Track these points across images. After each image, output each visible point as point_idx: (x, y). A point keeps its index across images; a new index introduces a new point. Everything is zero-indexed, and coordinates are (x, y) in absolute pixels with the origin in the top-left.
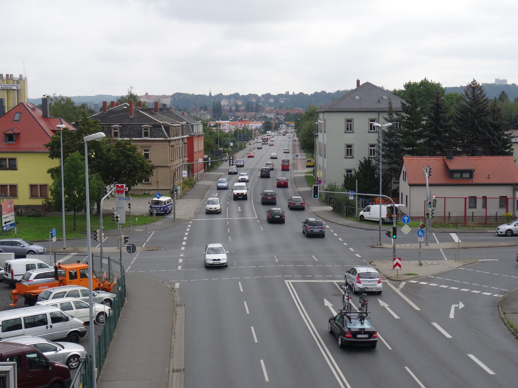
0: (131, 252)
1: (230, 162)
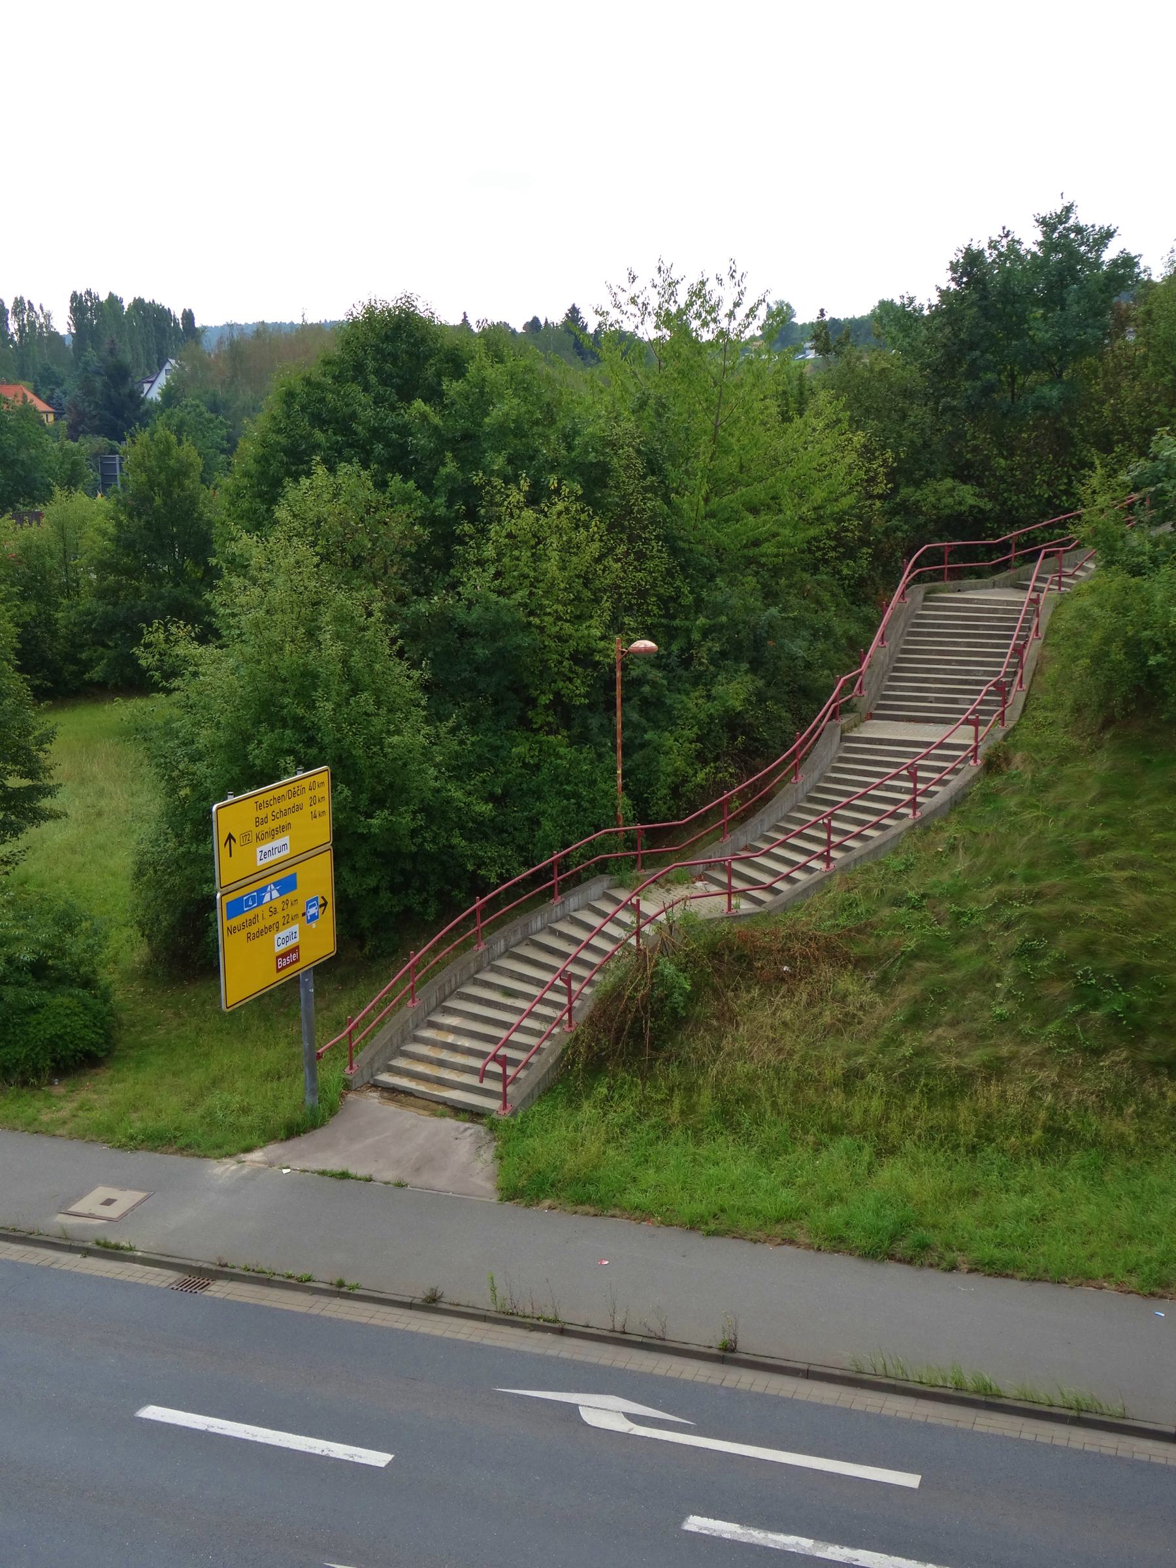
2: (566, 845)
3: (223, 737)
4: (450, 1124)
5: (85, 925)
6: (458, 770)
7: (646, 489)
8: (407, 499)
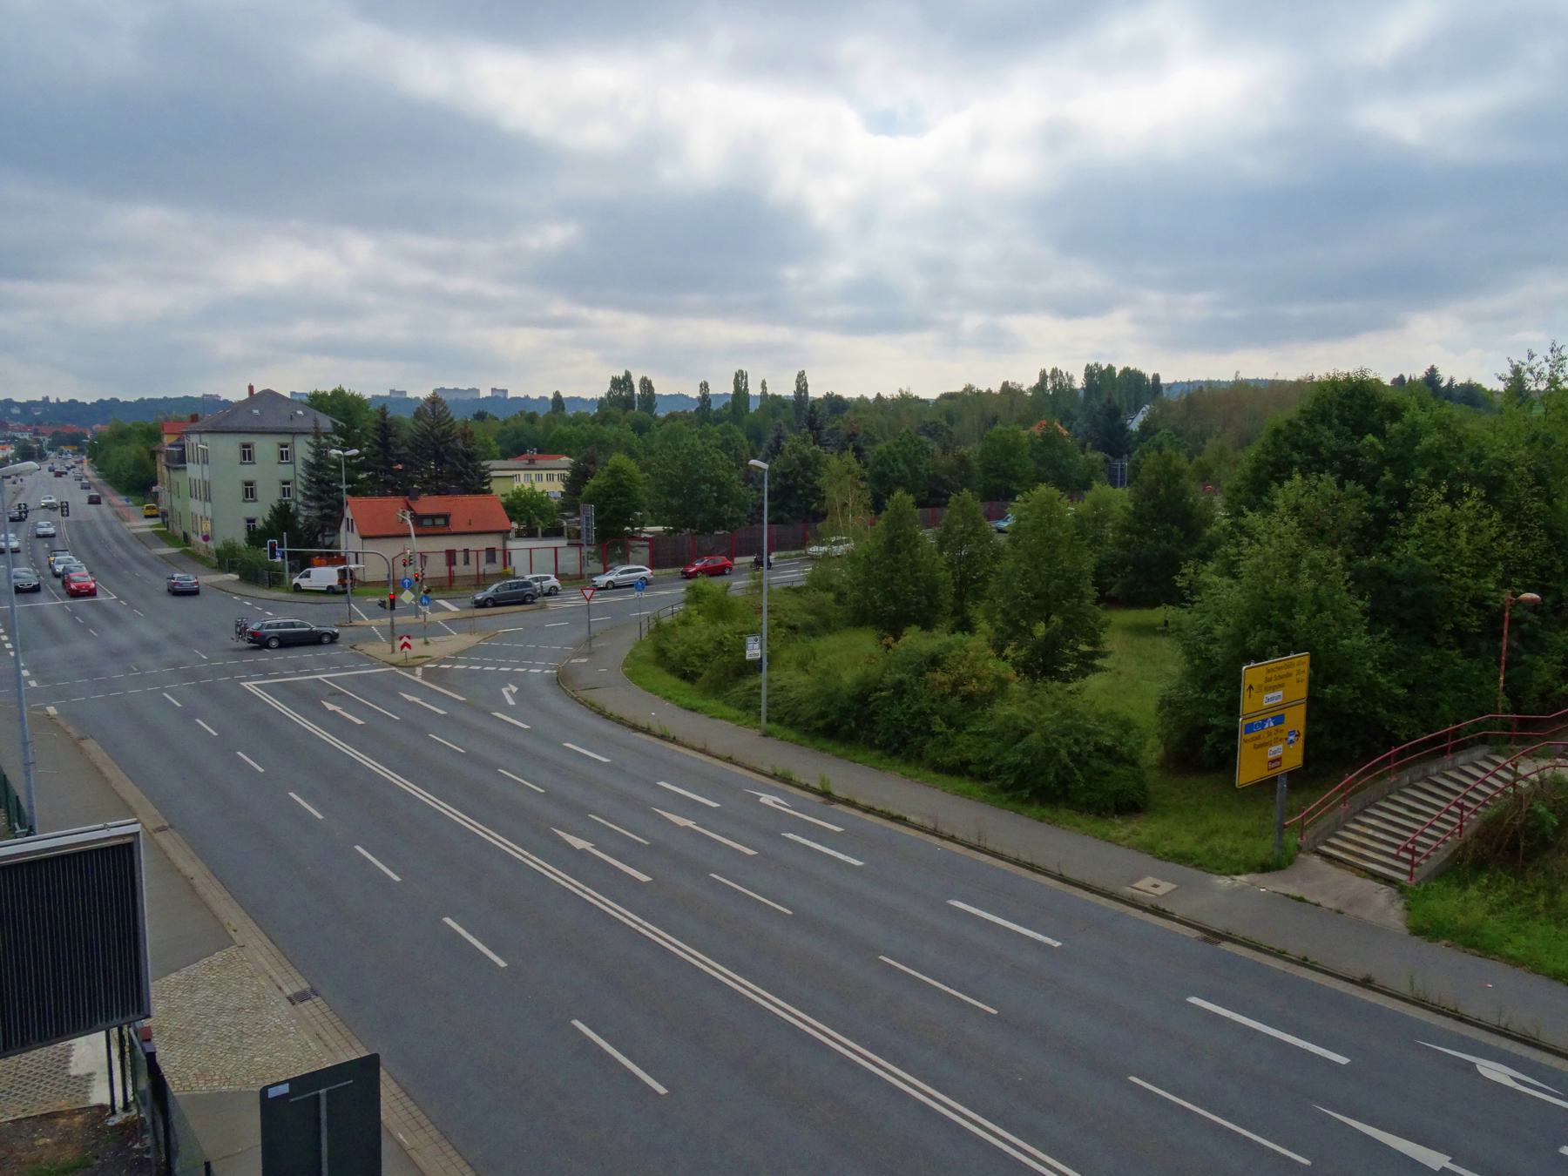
1: (62, 511)
2: (1458, 722)
3: (1230, 631)
4: (1370, 884)
5: (1135, 731)
6: (1387, 666)
7: (1534, 495)
8: (1357, 496)
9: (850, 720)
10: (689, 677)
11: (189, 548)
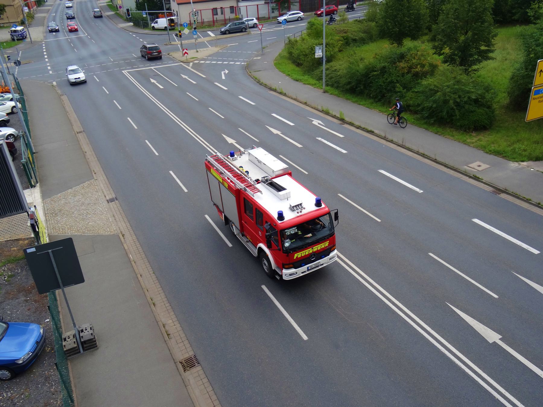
0: (18, 65)
5: (492, 91)
9: (361, 85)
10: (299, 65)
11: (118, 12)
